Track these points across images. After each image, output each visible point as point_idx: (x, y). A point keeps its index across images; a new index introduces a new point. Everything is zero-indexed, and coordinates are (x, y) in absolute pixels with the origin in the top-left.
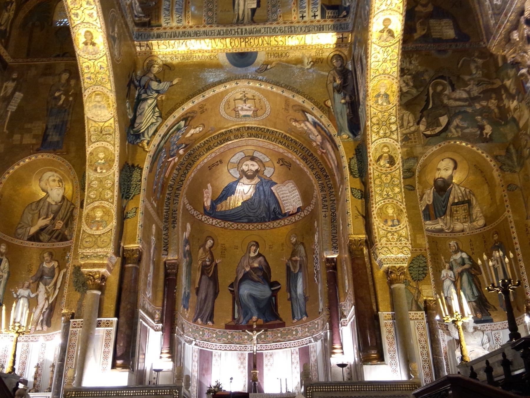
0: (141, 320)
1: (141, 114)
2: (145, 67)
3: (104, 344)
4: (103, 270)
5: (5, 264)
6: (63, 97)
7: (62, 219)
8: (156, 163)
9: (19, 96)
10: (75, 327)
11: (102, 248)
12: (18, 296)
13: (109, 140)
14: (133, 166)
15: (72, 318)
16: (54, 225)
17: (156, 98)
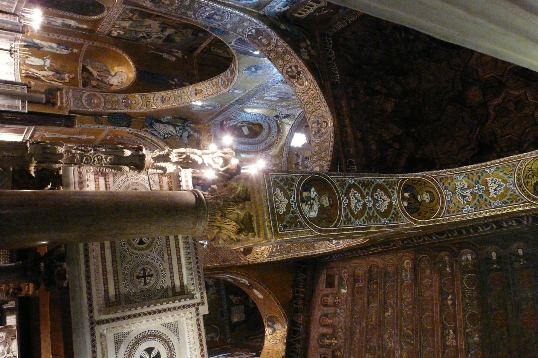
0: (27, 128)
1: (165, 126)
2: (197, 129)
3: (10, 105)
4: (59, 104)
5: (65, 52)
6: (174, 83)
7: (97, 84)
8: (134, 136)
9: (174, 59)
10: (21, 89)
11: (73, 103)
12: (45, 59)
13: (143, 106)
14: (130, 122)
15: (27, 87)
16: (94, 80)
17: (177, 136)
